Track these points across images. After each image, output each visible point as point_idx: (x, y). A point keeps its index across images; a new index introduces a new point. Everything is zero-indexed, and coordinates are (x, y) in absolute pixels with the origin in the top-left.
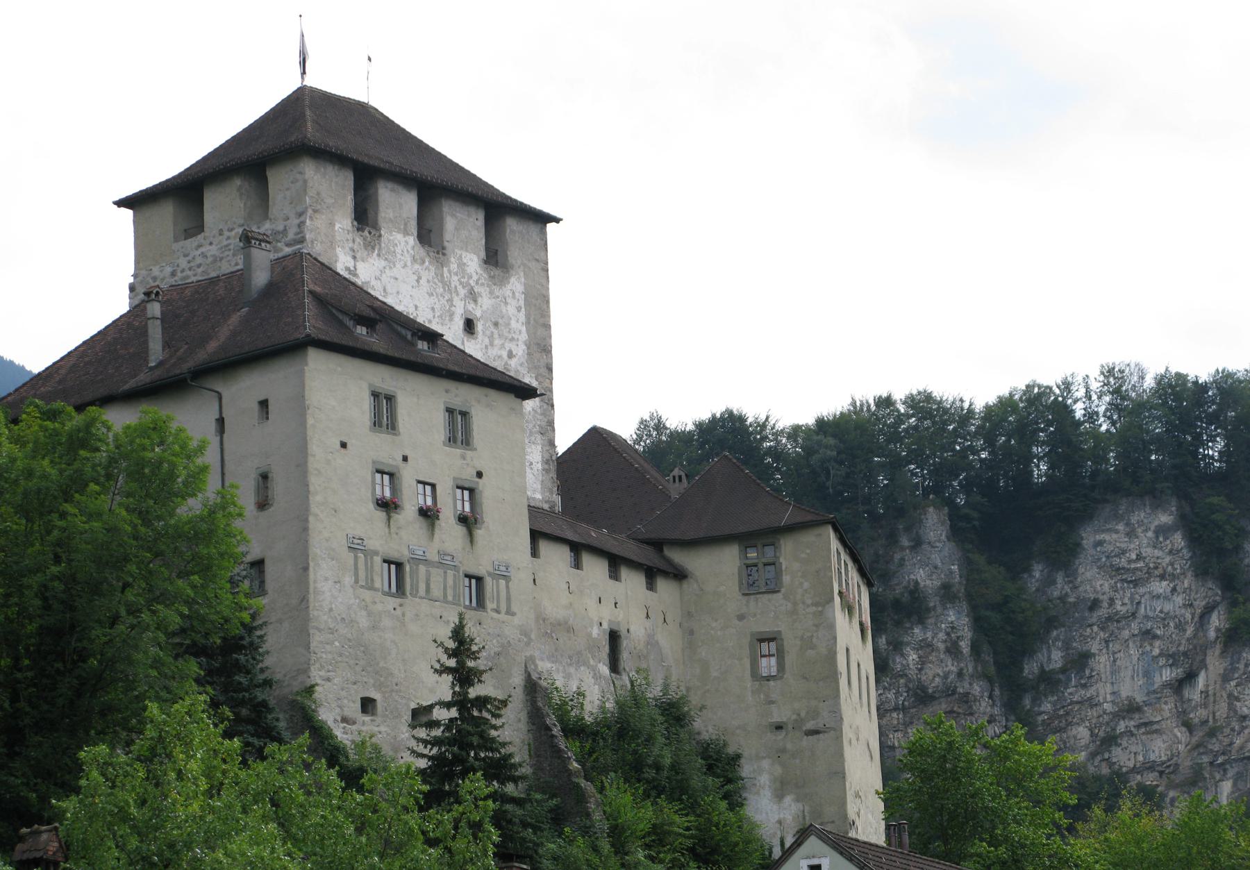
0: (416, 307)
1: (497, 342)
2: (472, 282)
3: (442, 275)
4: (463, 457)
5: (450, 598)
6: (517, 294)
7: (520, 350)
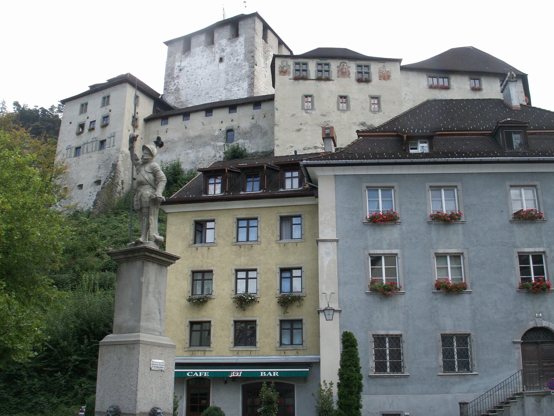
0: (202, 64)
1: (232, 59)
2: (223, 47)
3: (212, 51)
4: (106, 108)
5: (94, 150)
6: (241, 42)
7: (242, 57)
